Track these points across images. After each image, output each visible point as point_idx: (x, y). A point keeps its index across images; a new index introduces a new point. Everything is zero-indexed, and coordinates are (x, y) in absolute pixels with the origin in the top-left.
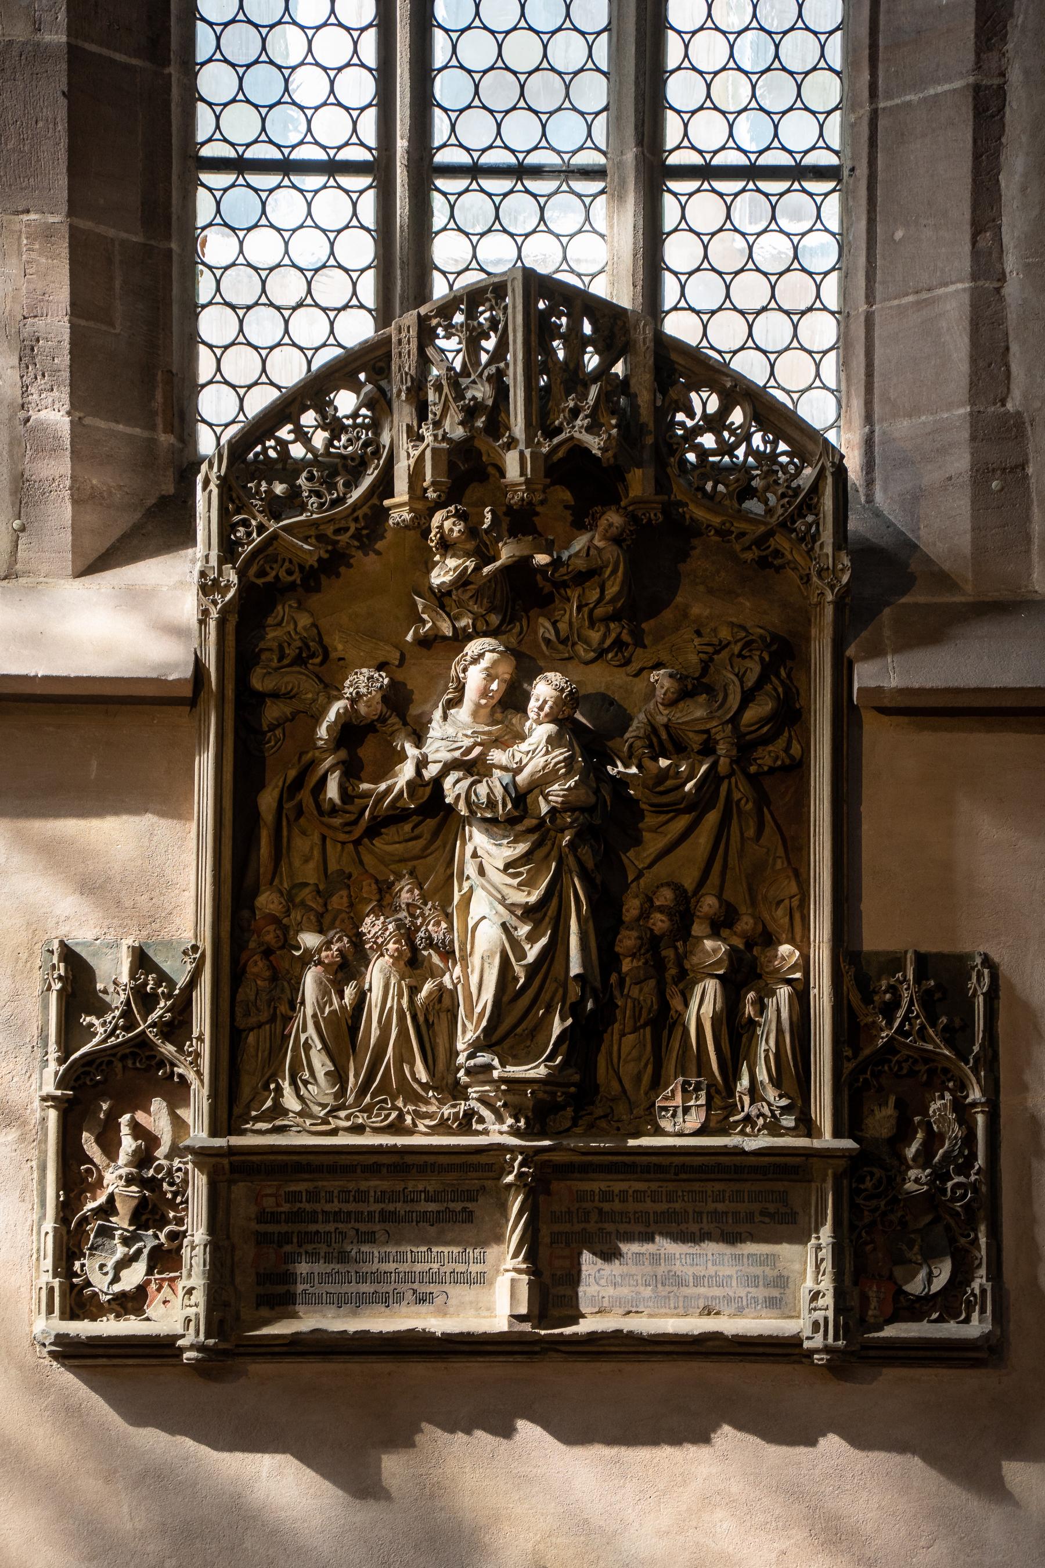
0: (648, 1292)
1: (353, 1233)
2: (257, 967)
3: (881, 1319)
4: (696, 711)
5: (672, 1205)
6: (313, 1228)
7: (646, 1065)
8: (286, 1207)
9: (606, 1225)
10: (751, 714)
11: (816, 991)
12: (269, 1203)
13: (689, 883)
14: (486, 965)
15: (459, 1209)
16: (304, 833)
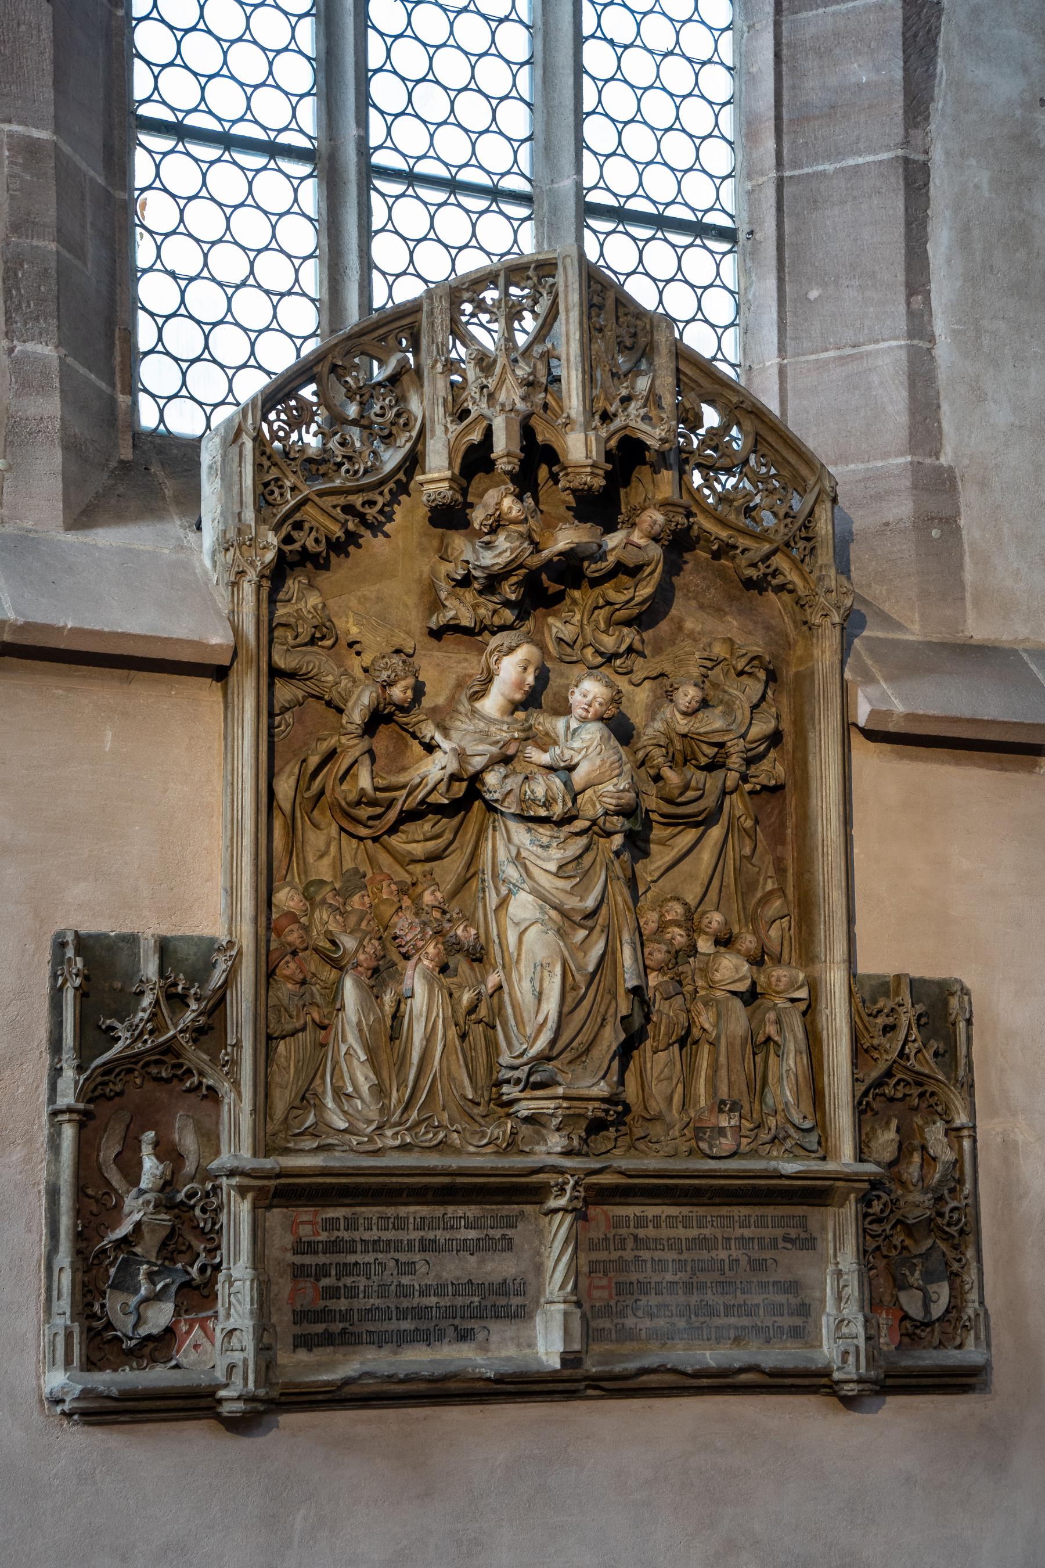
0: (681, 1323)
1: (392, 1263)
3: (893, 1347)
4: (713, 722)
5: (702, 1231)
6: (351, 1259)
8: (323, 1236)
9: (641, 1253)
11: (828, 1011)
12: (305, 1231)
13: (691, 899)
14: (546, 973)
15: (499, 1236)
16: (316, 826)
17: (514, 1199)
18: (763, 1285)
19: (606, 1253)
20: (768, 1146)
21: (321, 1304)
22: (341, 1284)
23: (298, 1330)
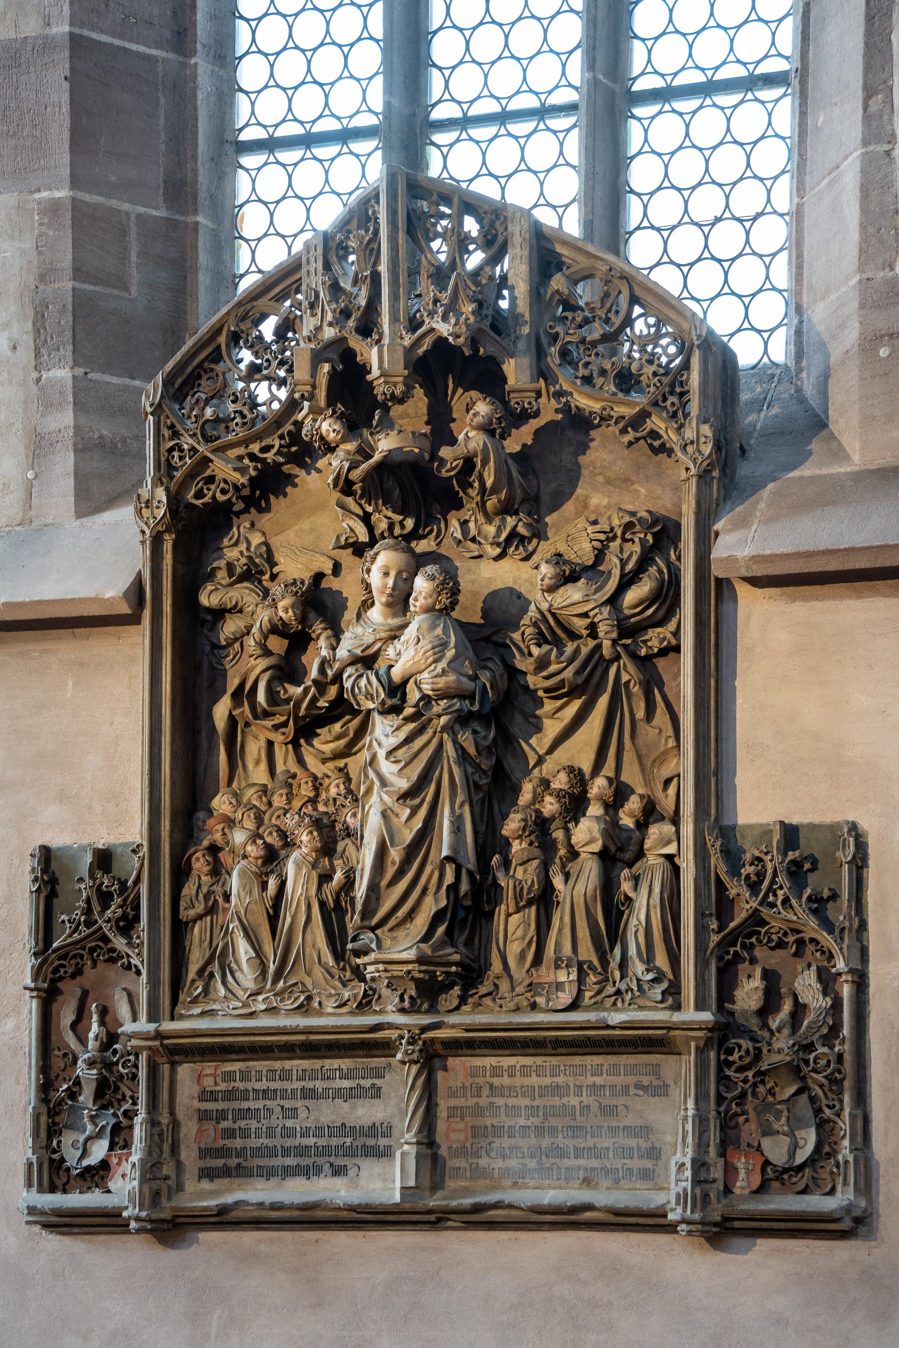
0: (532, 1164)
1: (279, 1109)
2: (200, 864)
3: (747, 1191)
5: (556, 1079)
6: (245, 1105)
7: (529, 944)
8: (223, 1086)
9: (496, 1100)
10: (632, 596)
12: (208, 1082)
13: (586, 765)
17: (373, 1052)
18: (613, 1130)
19: (463, 1100)
20: (613, 998)
21: (221, 1143)
22: (236, 1126)
23: (202, 1164)
